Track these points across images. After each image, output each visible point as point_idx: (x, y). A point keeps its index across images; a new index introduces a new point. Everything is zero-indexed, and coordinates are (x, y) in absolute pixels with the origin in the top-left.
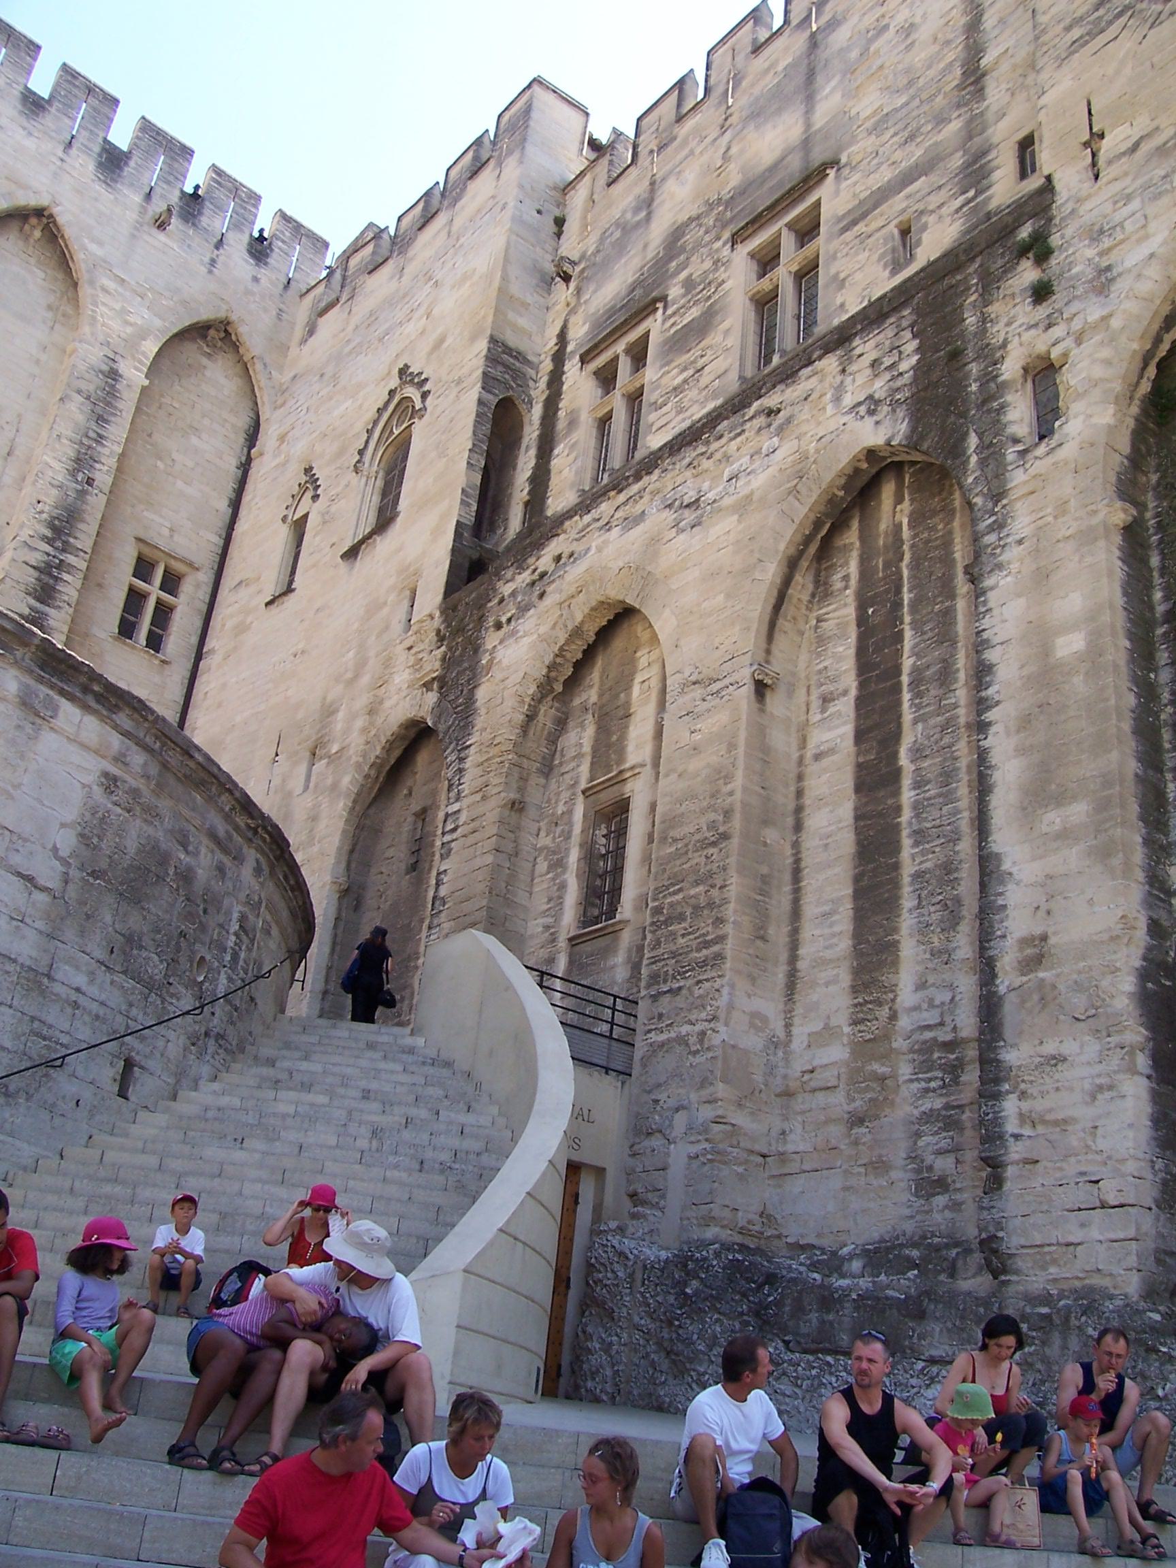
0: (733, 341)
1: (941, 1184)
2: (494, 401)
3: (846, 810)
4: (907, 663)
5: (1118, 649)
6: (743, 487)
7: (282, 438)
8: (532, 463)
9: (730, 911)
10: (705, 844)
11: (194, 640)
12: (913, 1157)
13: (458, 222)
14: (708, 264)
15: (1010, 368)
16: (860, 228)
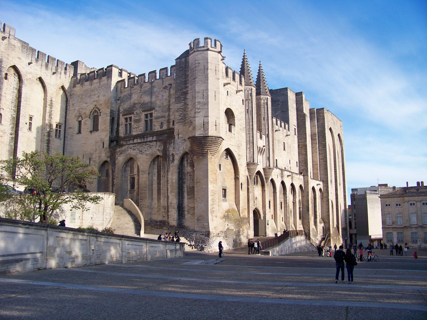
0: (143, 125)
1: (164, 217)
2: (111, 118)
3: (156, 185)
4: (162, 174)
5: (177, 182)
7: (73, 104)
8: (116, 126)
9: (147, 194)
10: (144, 187)
11: (64, 135)
12: (162, 214)
13: (101, 84)
14: (139, 112)
15: (171, 154)
16: (157, 120)
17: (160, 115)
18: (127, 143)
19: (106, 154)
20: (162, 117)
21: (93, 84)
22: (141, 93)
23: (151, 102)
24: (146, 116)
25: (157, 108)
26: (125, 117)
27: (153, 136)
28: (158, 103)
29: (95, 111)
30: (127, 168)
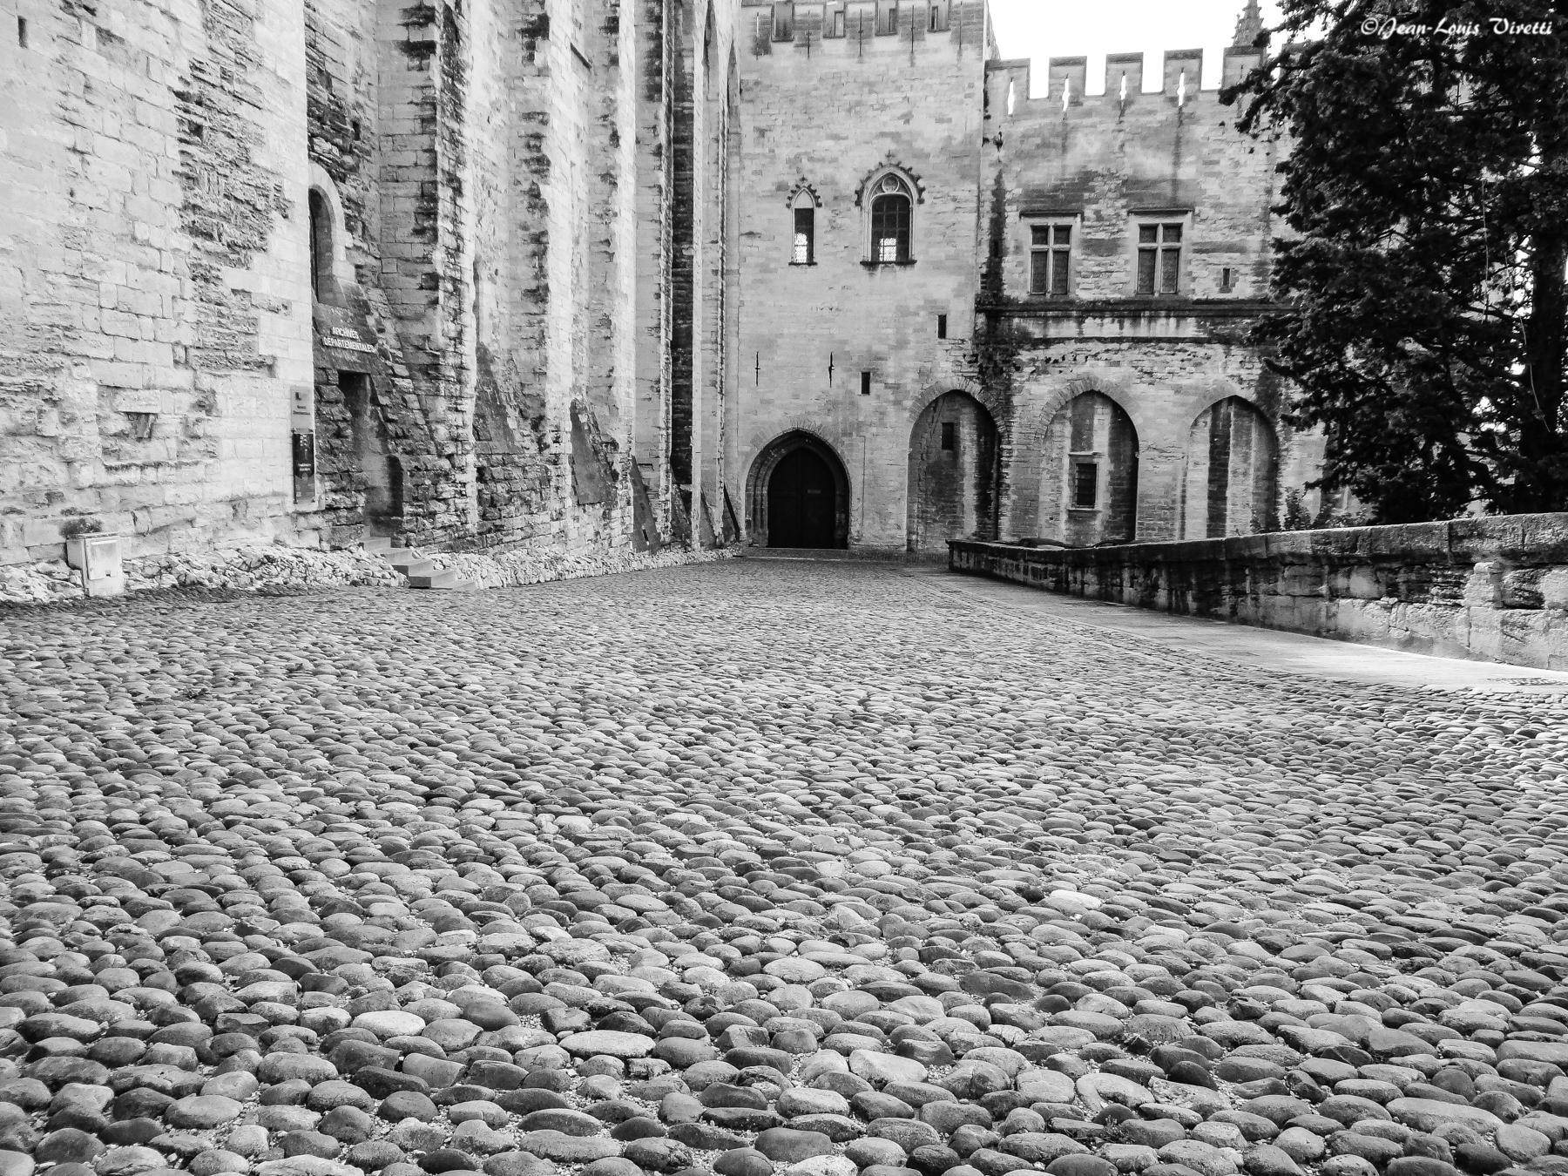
3: (1205, 503)
6: (1176, 381)
7: (762, 132)
13: (920, 60)
14: (1111, 212)
16: (1204, 256)
17: (1217, 238)
18: (1045, 326)
19: (958, 363)
20: (1230, 248)
21: (874, 55)
22: (1121, 136)
23: (1175, 183)
24: (1148, 232)
25: (1206, 211)
26: (1038, 221)
27: (1180, 318)
28: (1212, 187)
29: (892, 178)
30: (1057, 428)
